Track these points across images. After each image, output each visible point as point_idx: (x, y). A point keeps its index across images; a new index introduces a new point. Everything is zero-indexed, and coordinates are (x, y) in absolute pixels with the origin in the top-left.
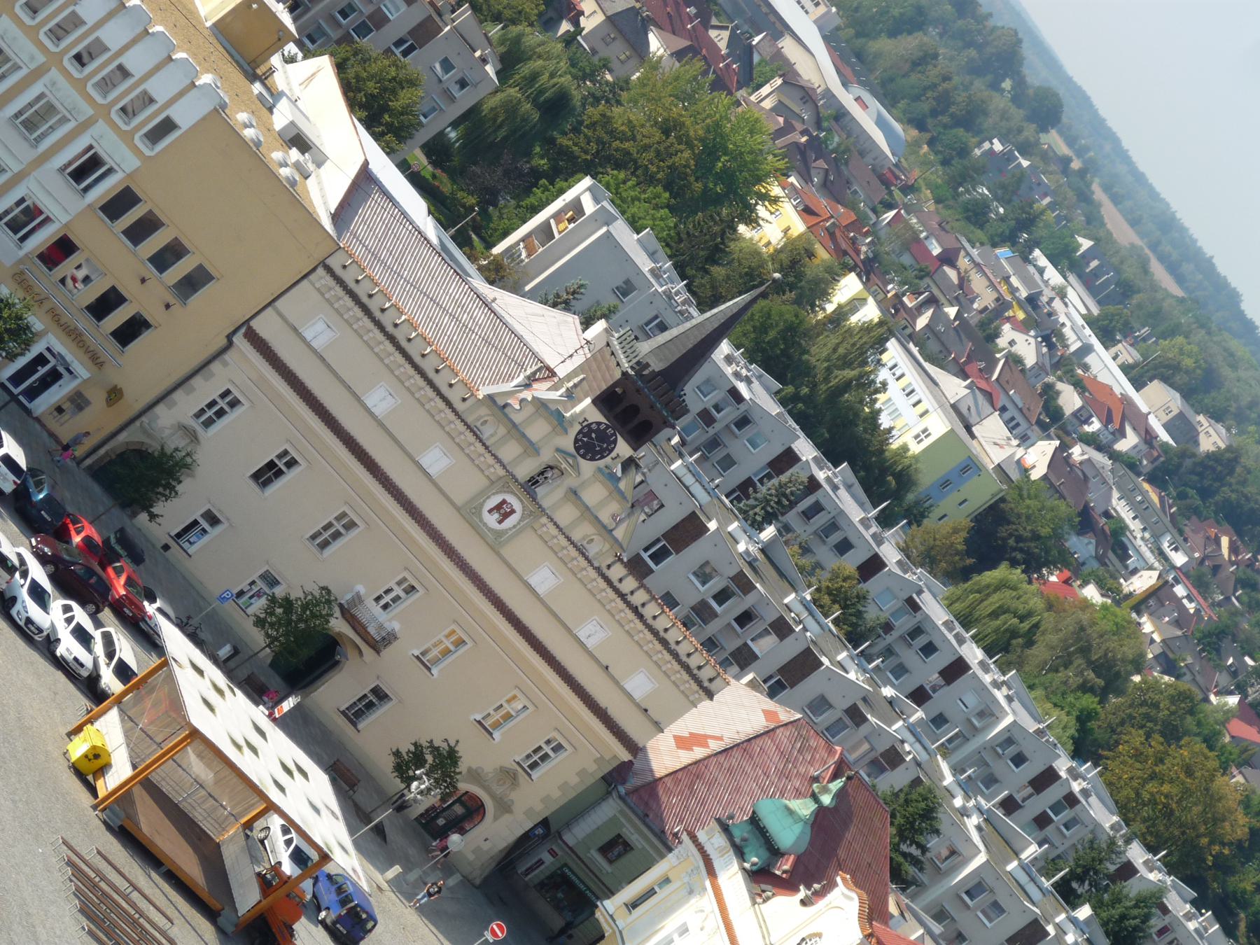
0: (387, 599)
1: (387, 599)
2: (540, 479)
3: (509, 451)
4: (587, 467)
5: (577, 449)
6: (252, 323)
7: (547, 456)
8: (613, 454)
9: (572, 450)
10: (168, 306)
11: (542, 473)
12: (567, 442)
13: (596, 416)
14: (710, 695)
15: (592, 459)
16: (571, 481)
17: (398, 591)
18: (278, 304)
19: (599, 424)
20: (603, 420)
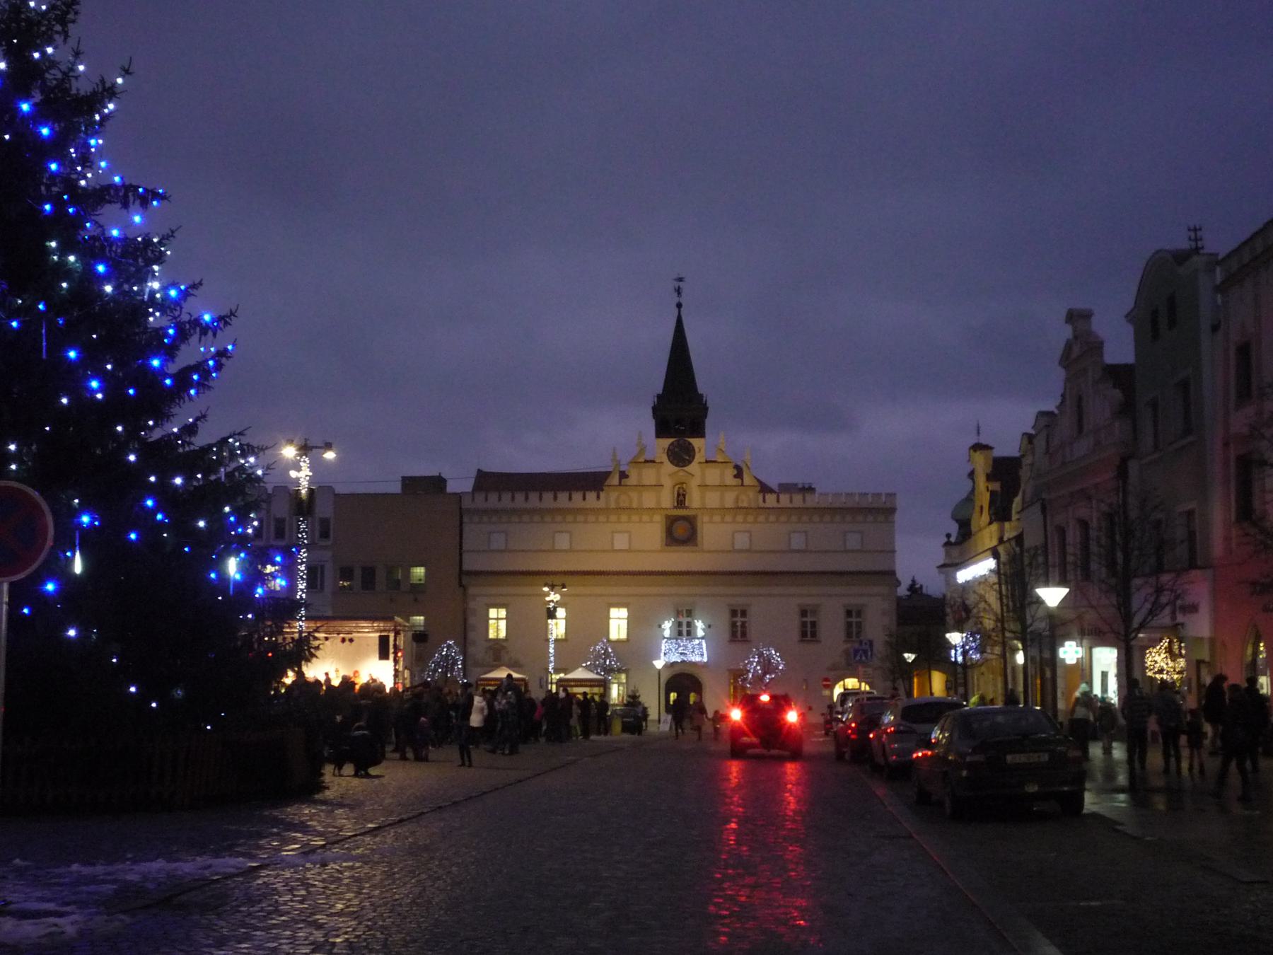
0: (684, 629)
1: (684, 629)
3: (649, 500)
4: (694, 467)
5: (677, 465)
6: (466, 567)
7: (668, 483)
9: (676, 469)
10: (416, 600)
12: (668, 467)
13: (667, 442)
14: (892, 510)
15: (690, 462)
16: (693, 485)
17: (684, 620)
18: (465, 547)
19: (672, 444)
20: (671, 440)
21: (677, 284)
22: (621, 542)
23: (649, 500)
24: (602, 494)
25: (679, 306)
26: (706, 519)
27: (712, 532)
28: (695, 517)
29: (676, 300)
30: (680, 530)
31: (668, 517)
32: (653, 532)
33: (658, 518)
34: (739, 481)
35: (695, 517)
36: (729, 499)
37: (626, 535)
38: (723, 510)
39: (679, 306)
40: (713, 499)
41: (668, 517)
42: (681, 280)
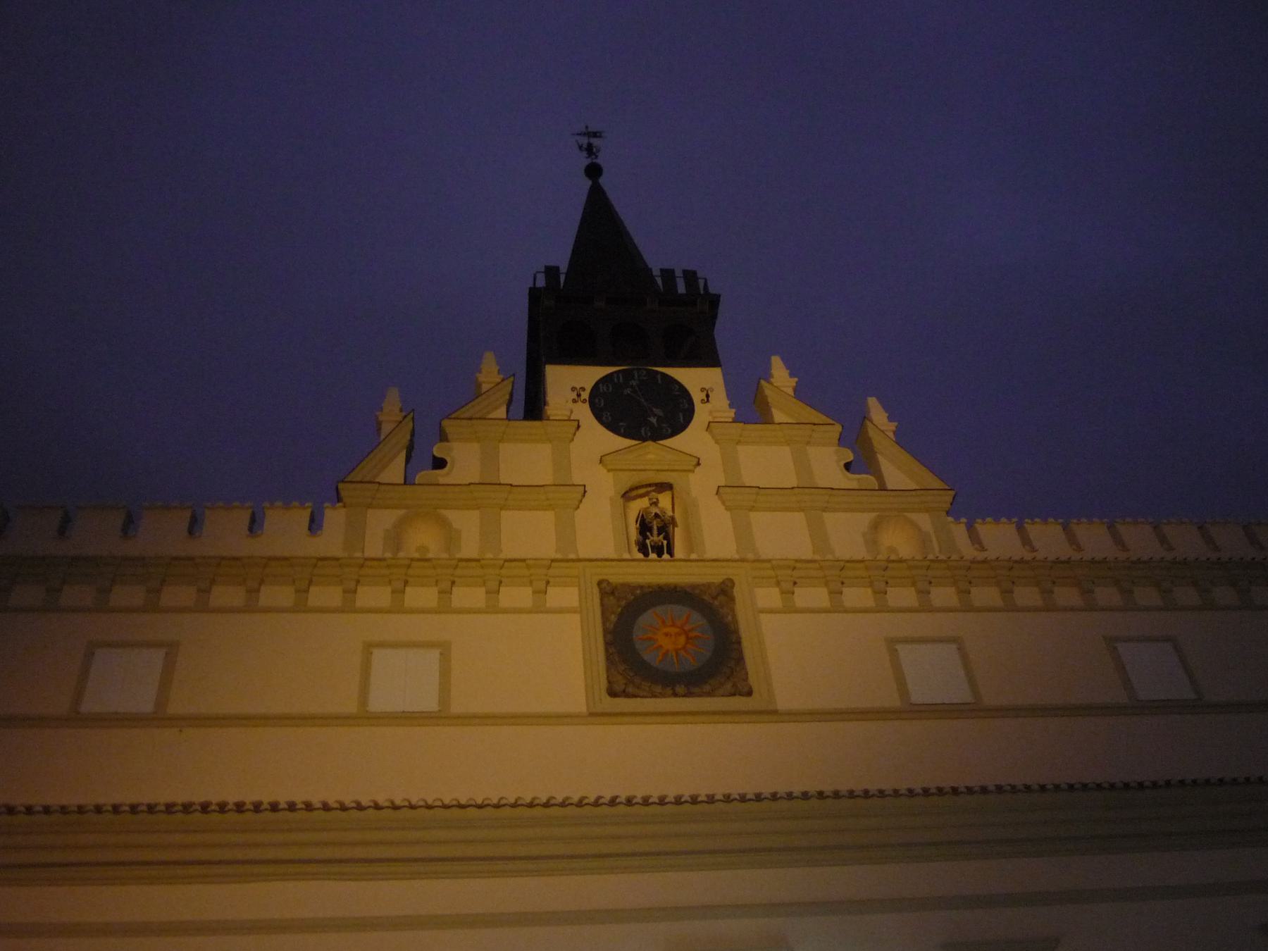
2: (655, 538)
8: (697, 397)
11: (644, 527)
21: (584, 141)
22: (403, 681)
23: (528, 533)
24: (334, 517)
25: (594, 171)
26: (768, 596)
27: (790, 644)
28: (725, 590)
29: (584, 161)
30: (665, 637)
31: (607, 591)
32: (555, 649)
33: (564, 596)
34: (870, 480)
35: (725, 590)
36: (847, 533)
37: (434, 654)
38: (835, 574)
39: (594, 171)
40: (781, 535)
41: (607, 591)
42: (595, 135)
